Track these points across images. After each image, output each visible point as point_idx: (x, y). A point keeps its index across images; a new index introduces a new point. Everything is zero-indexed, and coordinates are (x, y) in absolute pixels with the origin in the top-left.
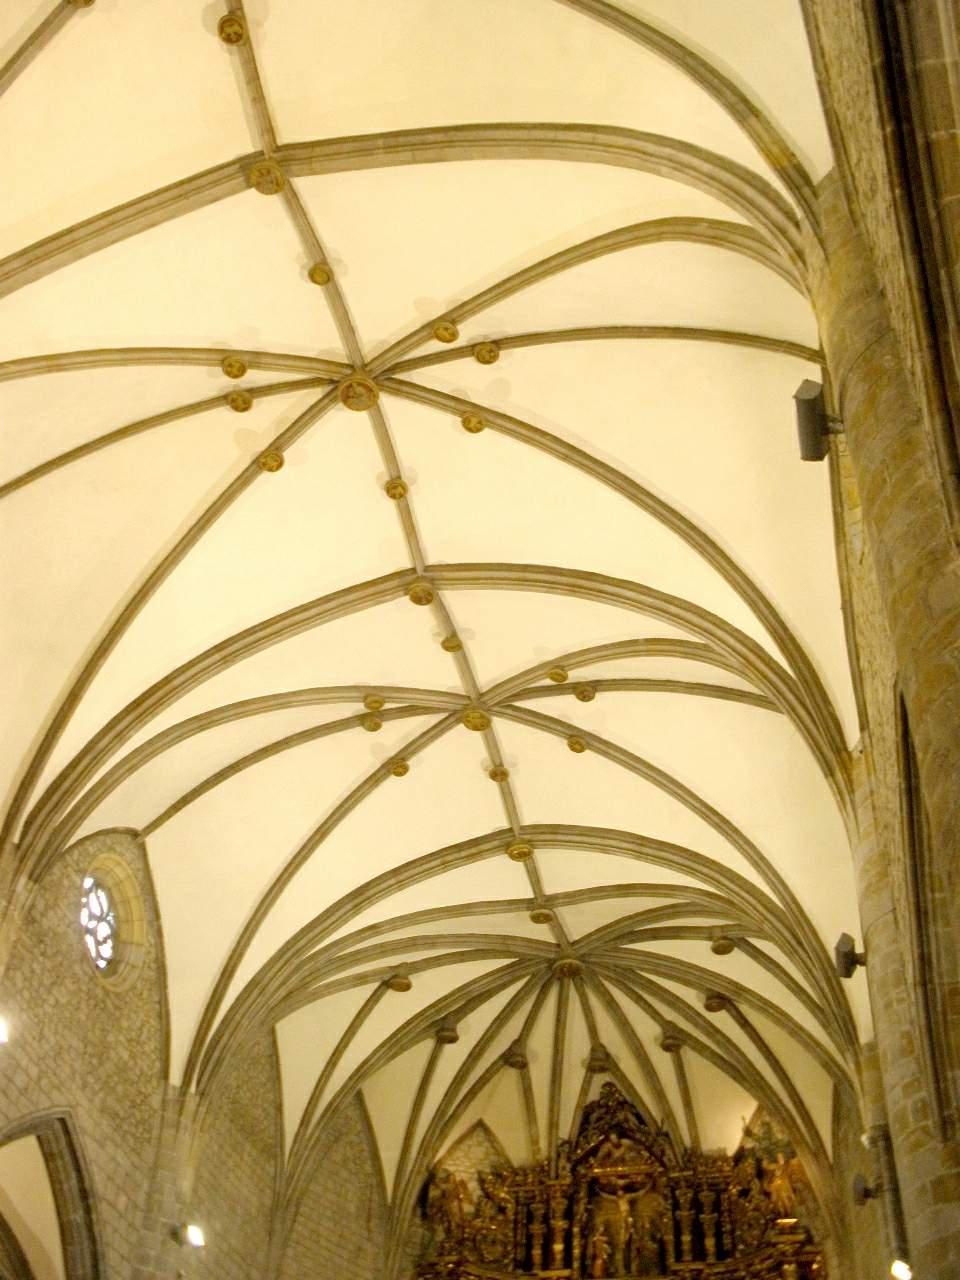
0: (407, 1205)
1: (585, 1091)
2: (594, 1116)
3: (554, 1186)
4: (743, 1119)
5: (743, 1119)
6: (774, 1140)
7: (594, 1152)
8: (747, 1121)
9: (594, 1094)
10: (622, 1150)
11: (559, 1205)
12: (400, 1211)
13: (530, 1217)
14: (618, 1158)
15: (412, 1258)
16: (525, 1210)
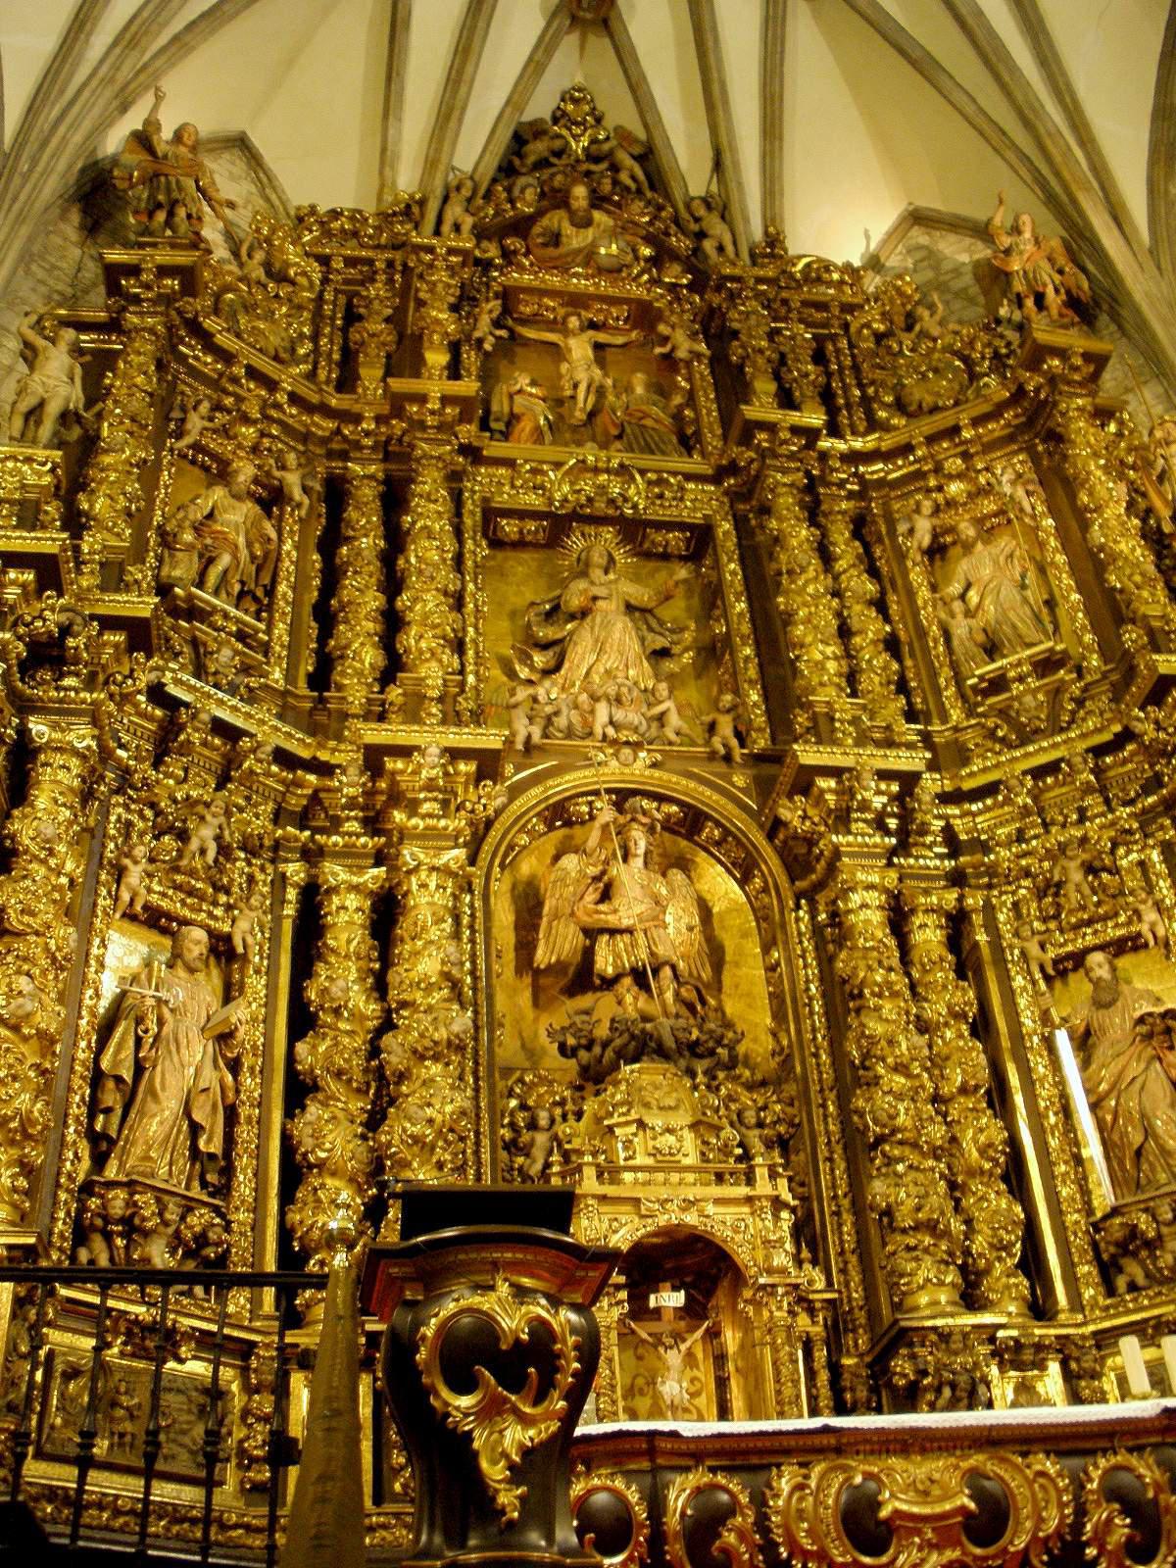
0: (64, 140)
1: (535, 66)
2: (538, 149)
3: (431, 250)
4: (868, 237)
5: (868, 237)
6: (946, 266)
7: (521, 226)
8: (873, 246)
9: (540, 106)
10: (590, 233)
11: (442, 282)
12: (34, 161)
13: (352, 317)
14: (579, 251)
15: (43, 289)
16: (342, 300)
